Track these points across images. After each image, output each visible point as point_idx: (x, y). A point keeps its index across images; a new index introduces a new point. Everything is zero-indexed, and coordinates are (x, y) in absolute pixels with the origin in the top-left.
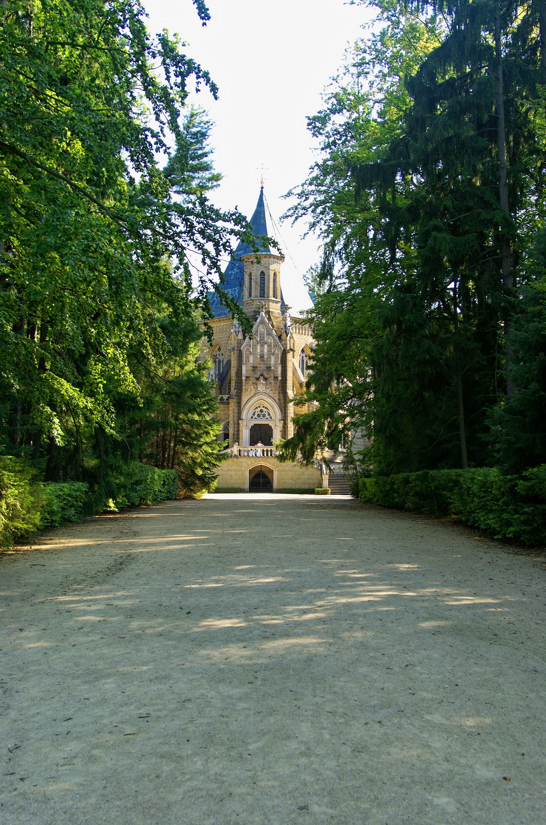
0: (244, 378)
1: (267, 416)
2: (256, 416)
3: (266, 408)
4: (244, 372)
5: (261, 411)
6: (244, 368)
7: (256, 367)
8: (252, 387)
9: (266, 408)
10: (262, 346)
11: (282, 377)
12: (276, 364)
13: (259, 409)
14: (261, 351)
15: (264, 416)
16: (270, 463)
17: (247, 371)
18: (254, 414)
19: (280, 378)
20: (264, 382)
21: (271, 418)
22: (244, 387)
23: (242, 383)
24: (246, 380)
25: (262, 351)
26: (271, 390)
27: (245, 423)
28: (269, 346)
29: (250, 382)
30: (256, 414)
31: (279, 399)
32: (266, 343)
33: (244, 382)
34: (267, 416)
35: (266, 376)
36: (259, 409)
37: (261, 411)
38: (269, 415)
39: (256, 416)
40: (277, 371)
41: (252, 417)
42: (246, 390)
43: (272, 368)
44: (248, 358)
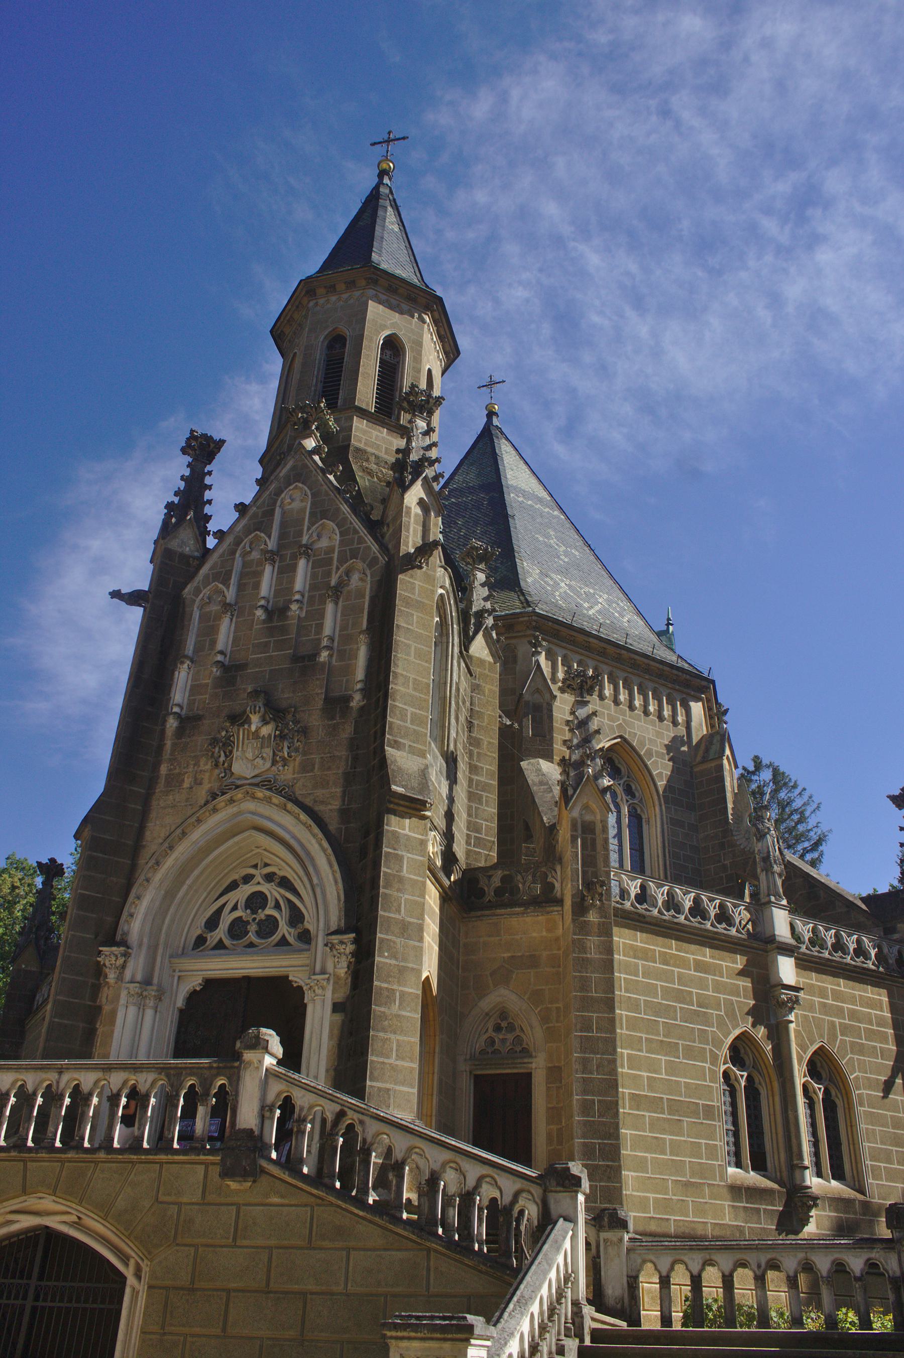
0: (172, 723)
1: (284, 929)
2: (221, 932)
3: (285, 883)
4: (179, 694)
5: (256, 901)
6: (182, 677)
7: (242, 667)
8: (206, 765)
9: (285, 883)
10: (287, 571)
11: (366, 692)
12: (347, 639)
13: (244, 892)
14: (277, 593)
15: (268, 927)
16: (104, 1210)
17: (195, 689)
18: (212, 923)
19: (357, 700)
20: (266, 731)
21: (305, 937)
22: (164, 769)
23: (160, 748)
24: (180, 732)
25: (283, 588)
26: (306, 767)
27: (136, 967)
28: (321, 563)
29: (200, 740)
30: (227, 919)
31: (344, 814)
32: (307, 550)
33: (168, 744)
34: (284, 929)
35: (285, 695)
36: (244, 892)
37: (256, 901)
38: (296, 917)
39: (221, 932)
40: (348, 670)
41: (200, 941)
42: (174, 781)
43: (324, 655)
44: (209, 631)
